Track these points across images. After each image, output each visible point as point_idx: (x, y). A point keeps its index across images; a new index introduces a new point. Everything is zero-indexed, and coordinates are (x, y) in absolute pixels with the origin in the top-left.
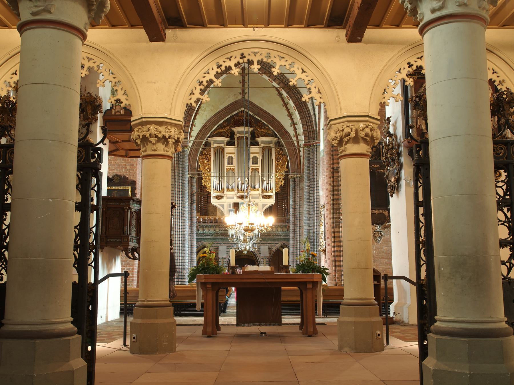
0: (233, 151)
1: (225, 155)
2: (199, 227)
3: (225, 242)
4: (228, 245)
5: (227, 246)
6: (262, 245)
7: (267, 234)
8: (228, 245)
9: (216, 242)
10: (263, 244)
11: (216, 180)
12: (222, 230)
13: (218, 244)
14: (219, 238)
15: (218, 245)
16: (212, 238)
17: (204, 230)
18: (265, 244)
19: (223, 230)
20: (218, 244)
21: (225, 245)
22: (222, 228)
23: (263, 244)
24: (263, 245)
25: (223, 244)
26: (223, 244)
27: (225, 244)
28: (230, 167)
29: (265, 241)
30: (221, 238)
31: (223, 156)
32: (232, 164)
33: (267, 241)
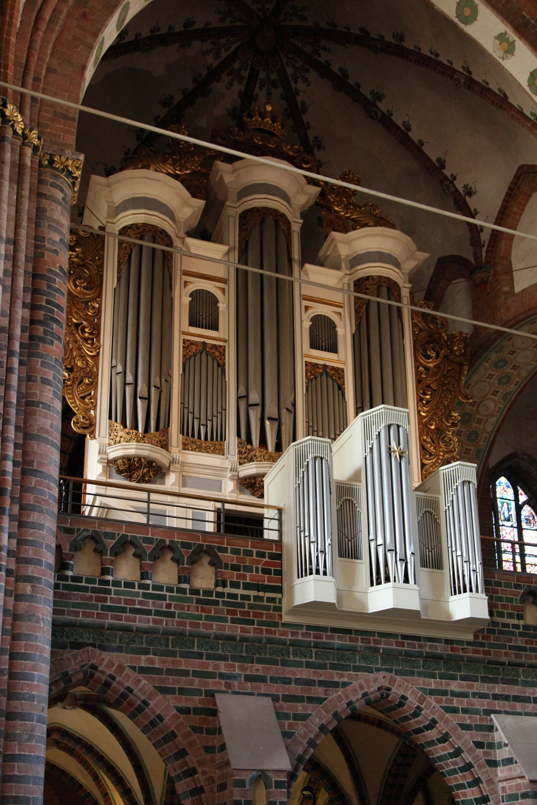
0: (219, 271)
1: (178, 279)
2: (66, 550)
3: (258, 669)
4: (279, 689)
5: (275, 698)
6: (498, 705)
7: (520, 642)
8: (279, 689)
9: (194, 665)
10: (507, 698)
11: (130, 378)
12: (235, 585)
13: (211, 675)
14: (217, 637)
15: (211, 684)
16: (166, 633)
17: (105, 571)
18: (517, 699)
19: (247, 586)
20: (211, 675)
21: (263, 688)
22: (236, 568)
23: (507, 698)
24: (506, 705)
25: (248, 678)
26: (248, 678)
27: (261, 679)
28: (202, 340)
29: (514, 682)
30: (231, 638)
31: (171, 278)
32: (215, 327)
33: (526, 684)
